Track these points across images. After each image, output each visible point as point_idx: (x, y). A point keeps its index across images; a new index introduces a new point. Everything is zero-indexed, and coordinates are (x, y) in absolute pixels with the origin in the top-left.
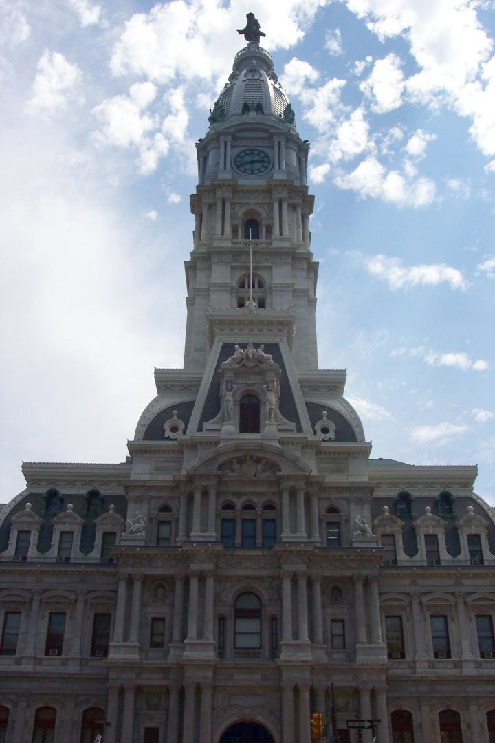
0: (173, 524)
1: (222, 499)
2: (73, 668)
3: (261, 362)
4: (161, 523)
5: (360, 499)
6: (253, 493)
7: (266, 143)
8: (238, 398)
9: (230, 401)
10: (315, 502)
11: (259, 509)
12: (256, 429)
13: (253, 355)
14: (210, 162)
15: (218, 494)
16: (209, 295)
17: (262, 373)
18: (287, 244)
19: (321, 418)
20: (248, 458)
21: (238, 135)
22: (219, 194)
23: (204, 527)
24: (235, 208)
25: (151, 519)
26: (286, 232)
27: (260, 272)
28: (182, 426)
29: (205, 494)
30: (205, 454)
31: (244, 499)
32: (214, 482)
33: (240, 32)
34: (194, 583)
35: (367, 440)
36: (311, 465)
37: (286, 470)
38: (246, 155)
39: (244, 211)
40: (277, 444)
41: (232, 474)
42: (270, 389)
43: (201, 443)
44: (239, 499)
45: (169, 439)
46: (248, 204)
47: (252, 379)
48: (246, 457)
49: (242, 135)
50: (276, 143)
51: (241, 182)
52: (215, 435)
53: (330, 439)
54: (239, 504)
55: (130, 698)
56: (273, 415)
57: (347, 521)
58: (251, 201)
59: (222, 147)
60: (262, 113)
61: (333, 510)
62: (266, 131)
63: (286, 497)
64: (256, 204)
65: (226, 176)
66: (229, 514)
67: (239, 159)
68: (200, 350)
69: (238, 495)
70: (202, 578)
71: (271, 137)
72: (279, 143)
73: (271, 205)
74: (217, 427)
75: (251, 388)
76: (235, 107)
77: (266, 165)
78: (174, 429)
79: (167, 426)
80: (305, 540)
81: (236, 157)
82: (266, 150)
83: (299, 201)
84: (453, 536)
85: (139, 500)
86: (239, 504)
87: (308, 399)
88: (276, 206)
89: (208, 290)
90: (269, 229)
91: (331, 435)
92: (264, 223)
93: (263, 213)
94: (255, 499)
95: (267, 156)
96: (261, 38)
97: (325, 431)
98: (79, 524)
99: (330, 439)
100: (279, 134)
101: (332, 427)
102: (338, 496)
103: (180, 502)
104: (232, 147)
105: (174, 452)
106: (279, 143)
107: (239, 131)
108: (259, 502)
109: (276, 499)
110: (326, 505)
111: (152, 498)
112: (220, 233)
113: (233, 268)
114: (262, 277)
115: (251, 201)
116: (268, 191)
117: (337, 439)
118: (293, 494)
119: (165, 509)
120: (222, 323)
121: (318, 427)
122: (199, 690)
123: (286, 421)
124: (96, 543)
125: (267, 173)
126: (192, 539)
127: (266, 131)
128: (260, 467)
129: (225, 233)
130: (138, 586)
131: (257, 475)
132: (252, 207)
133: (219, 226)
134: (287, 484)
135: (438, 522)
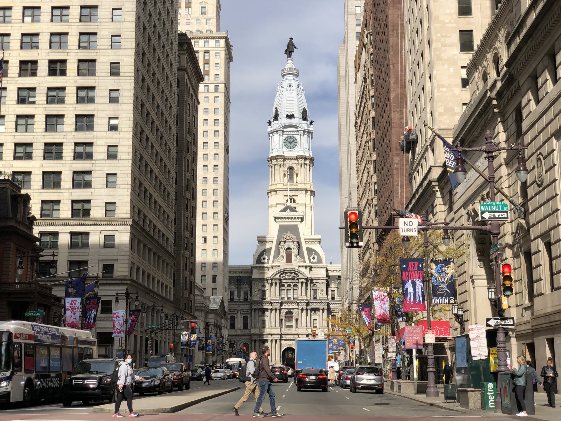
2: (239, 332)
9: (283, 252)
15: (280, 283)
29: (276, 284)
30: (275, 270)
32: (278, 281)
34: (274, 311)
36: (307, 273)
40: (297, 268)
54: (286, 285)
55: (257, 343)
66: (283, 288)
70: (276, 310)
79: (262, 258)
87: (308, 246)
91: (315, 260)
94: (291, 284)
97: (314, 258)
108: (292, 284)
109: (297, 284)
118: (302, 283)
121: (311, 258)
122: (276, 340)
130: (257, 311)
134: (300, 281)
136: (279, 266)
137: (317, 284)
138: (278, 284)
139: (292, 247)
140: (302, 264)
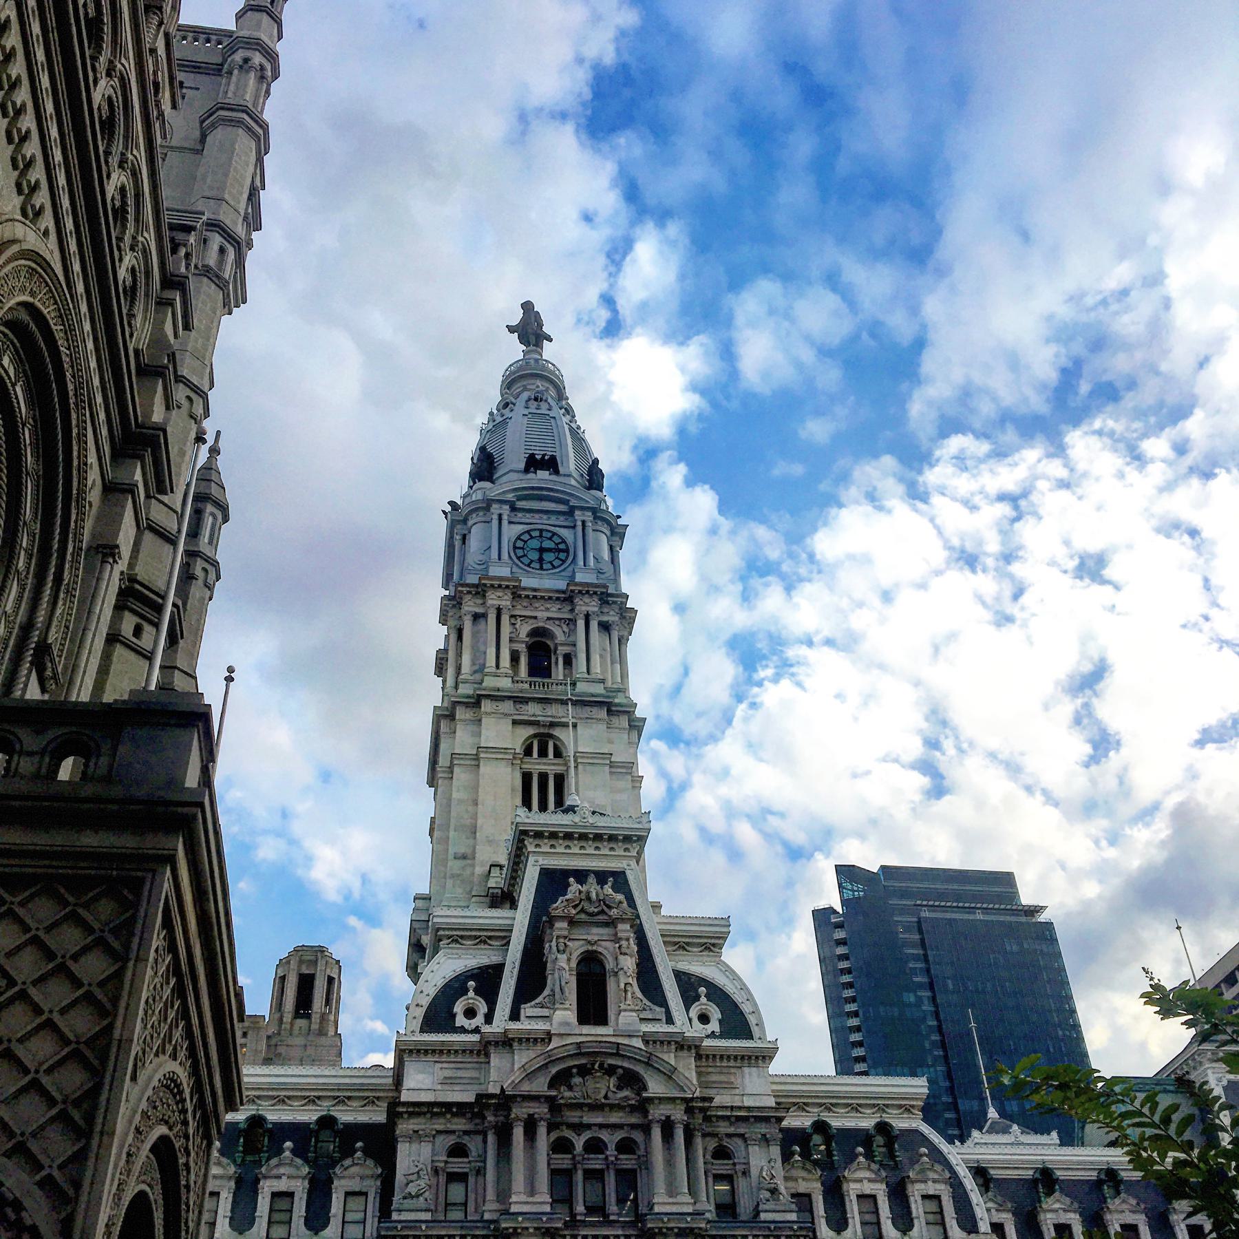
0: (471, 1180)
1: (554, 1136)
3: (610, 907)
4: (453, 1177)
5: (764, 1135)
6: (601, 1126)
7: (561, 520)
8: (574, 964)
10: (699, 1141)
11: (611, 1151)
12: (602, 1020)
13: (597, 895)
16: (478, 766)
17: (611, 923)
18: (598, 689)
19: (697, 998)
20: (596, 1067)
21: (520, 504)
22: (493, 599)
23: (532, 1191)
24: (514, 624)
25: (436, 1171)
26: (597, 668)
27: (557, 732)
28: (482, 1008)
31: (587, 1135)
32: (541, 1110)
33: (511, 329)
35: (770, 1037)
37: (655, 1087)
38: (532, 537)
39: (529, 628)
40: (638, 1043)
41: (567, 1094)
42: (623, 950)
43: (520, 1040)
44: (579, 1135)
45: (463, 1030)
46: (535, 618)
47: (596, 933)
48: (593, 1065)
49: (520, 504)
50: (579, 523)
51: (528, 581)
52: (541, 1026)
53: (712, 1035)
54: (579, 1143)
56: (629, 995)
57: (746, 1173)
59: (495, 523)
60: (557, 472)
61: (721, 1153)
62: (566, 502)
63: (657, 1133)
64: (549, 619)
65: (501, 571)
66: (563, 1161)
67: (520, 544)
68: (464, 857)
69: (579, 1128)
71: (570, 512)
73: (572, 622)
74: (545, 1012)
75: (594, 948)
76: (513, 457)
77: (562, 556)
78: (470, 1013)
79: (459, 1008)
80: (690, 1209)
81: (515, 541)
82: (565, 533)
84: (898, 1194)
85: (416, 1136)
86: (579, 1143)
88: (581, 623)
89: (477, 758)
90: (568, 660)
92: (562, 650)
93: (559, 634)
94: (604, 1135)
95: (564, 542)
98: (304, 1178)
99: (712, 1035)
100: (582, 509)
101: (715, 1014)
102: (732, 1130)
103: (485, 1141)
104: (510, 522)
105: (471, 1052)
107: (520, 498)
109: (638, 1136)
110: (712, 1144)
111: (439, 1132)
112: (494, 665)
113: (515, 723)
114: (563, 744)
115: (539, 614)
116: (567, 598)
117: (722, 1035)
118: (668, 1127)
119: (458, 1151)
120: (539, 835)
121: (694, 1011)
123: (648, 1003)
124: (333, 1211)
126: (514, 1209)
127: (566, 502)
128: (613, 1081)
129: (502, 665)
131: (610, 1094)
132: (541, 624)
133: (491, 652)
134: (657, 1112)
135: (877, 1173)
136: (548, 1036)
137: (736, 1145)
138: (542, 1130)
139: (606, 949)
140: (662, 1028)
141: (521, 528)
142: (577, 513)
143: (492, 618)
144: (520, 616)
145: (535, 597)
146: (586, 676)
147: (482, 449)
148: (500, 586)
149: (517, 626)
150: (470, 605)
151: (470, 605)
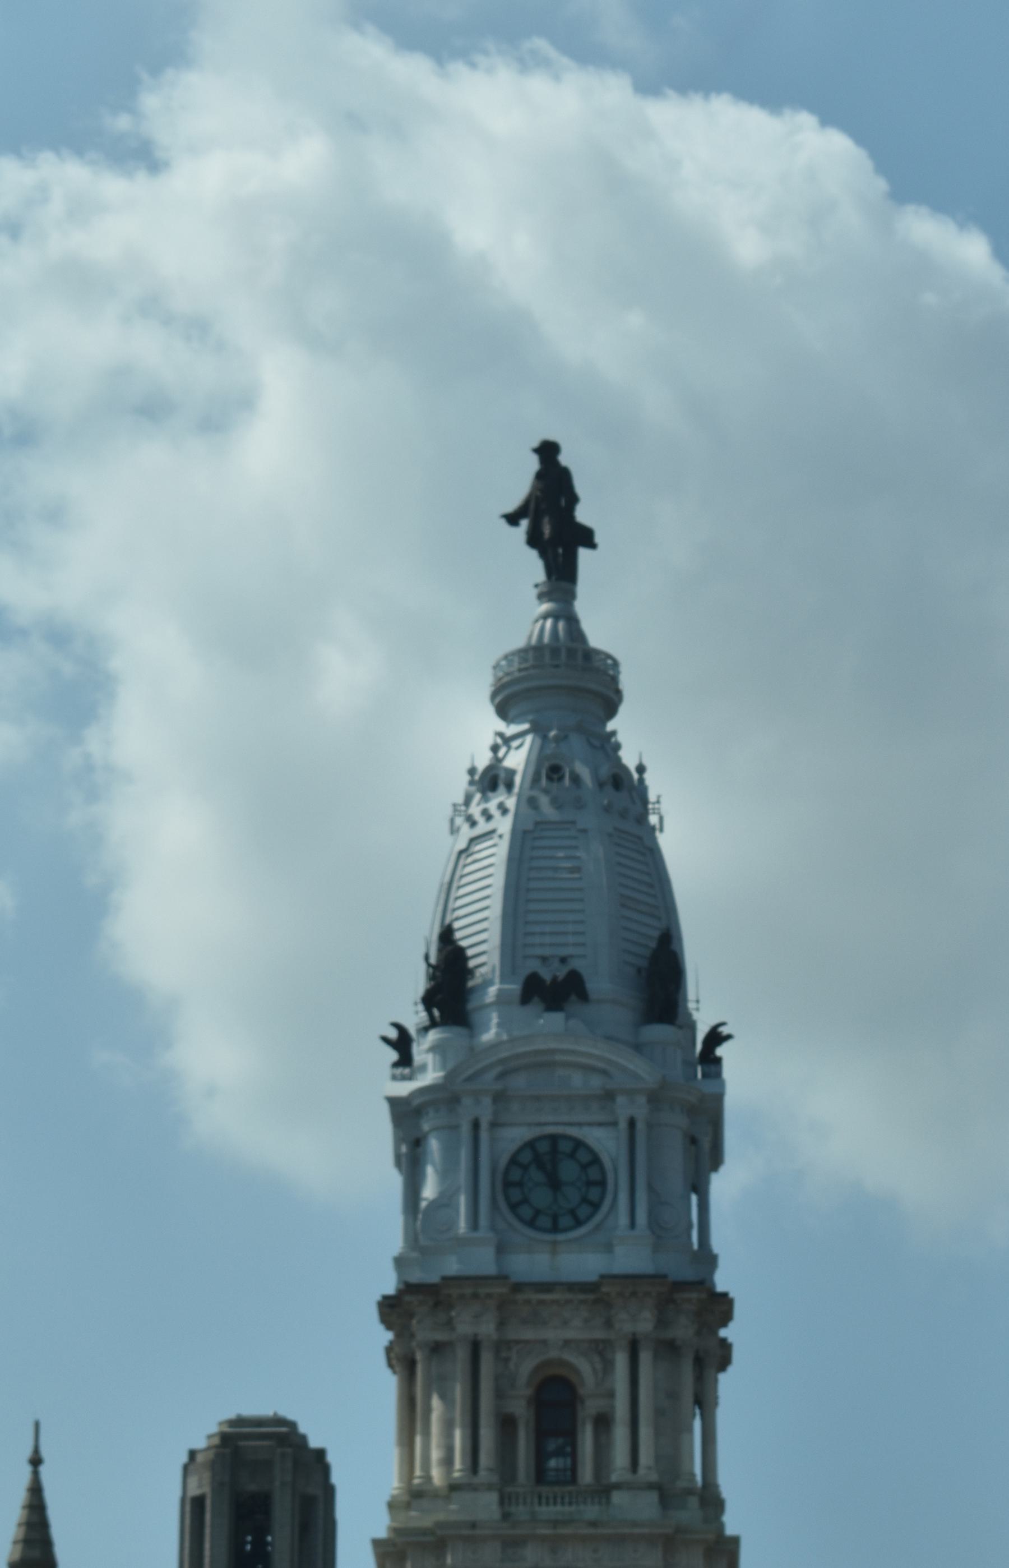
14: (429, 1191)
24: (507, 1360)
26: (645, 1457)
33: (513, 519)
46: (544, 1342)
49: (519, 1082)
50: (623, 1125)
58: (551, 1334)
64: (567, 1343)
67: (516, 1175)
71: (609, 1096)
72: (632, 1123)
83: (683, 1330)
88: (621, 1361)
90: (603, 1422)
92: (591, 1407)
96: (584, 554)
106: (632, 1123)
125: (598, 1227)
132: (553, 1354)
141: (515, 1136)
142: (621, 1100)
143: (462, 1354)
144: (517, 1342)
145: (542, 1302)
146: (628, 1476)
147: (447, 935)
148: (475, 1296)
149: (512, 1365)
150: (425, 1332)
151: (425, 1332)
